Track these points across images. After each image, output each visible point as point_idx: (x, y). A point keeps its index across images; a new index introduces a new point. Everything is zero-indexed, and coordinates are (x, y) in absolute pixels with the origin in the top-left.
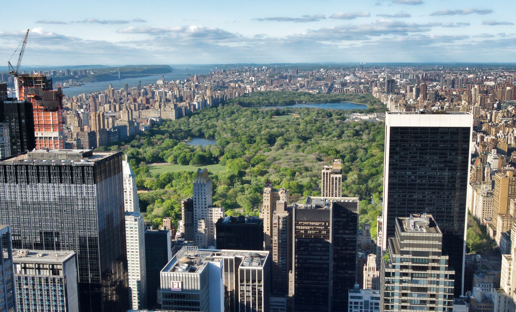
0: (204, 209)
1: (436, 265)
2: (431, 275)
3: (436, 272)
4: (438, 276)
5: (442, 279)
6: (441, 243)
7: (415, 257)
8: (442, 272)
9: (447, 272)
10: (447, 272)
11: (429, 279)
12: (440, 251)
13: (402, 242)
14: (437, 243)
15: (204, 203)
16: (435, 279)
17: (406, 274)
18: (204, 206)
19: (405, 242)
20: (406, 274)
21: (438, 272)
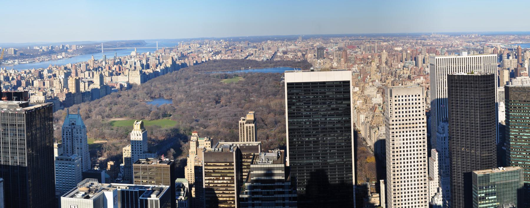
0: (140, 154)
1: (281, 190)
2: (277, 199)
3: (281, 196)
4: (284, 199)
5: (287, 201)
6: (284, 172)
7: (263, 185)
8: (287, 196)
9: (290, 196)
10: (290, 196)
11: (277, 202)
12: (284, 178)
13: (252, 173)
14: (280, 172)
15: (139, 149)
16: (281, 202)
17: (257, 199)
18: (139, 152)
19: (255, 172)
20: (257, 199)
21: (284, 196)
